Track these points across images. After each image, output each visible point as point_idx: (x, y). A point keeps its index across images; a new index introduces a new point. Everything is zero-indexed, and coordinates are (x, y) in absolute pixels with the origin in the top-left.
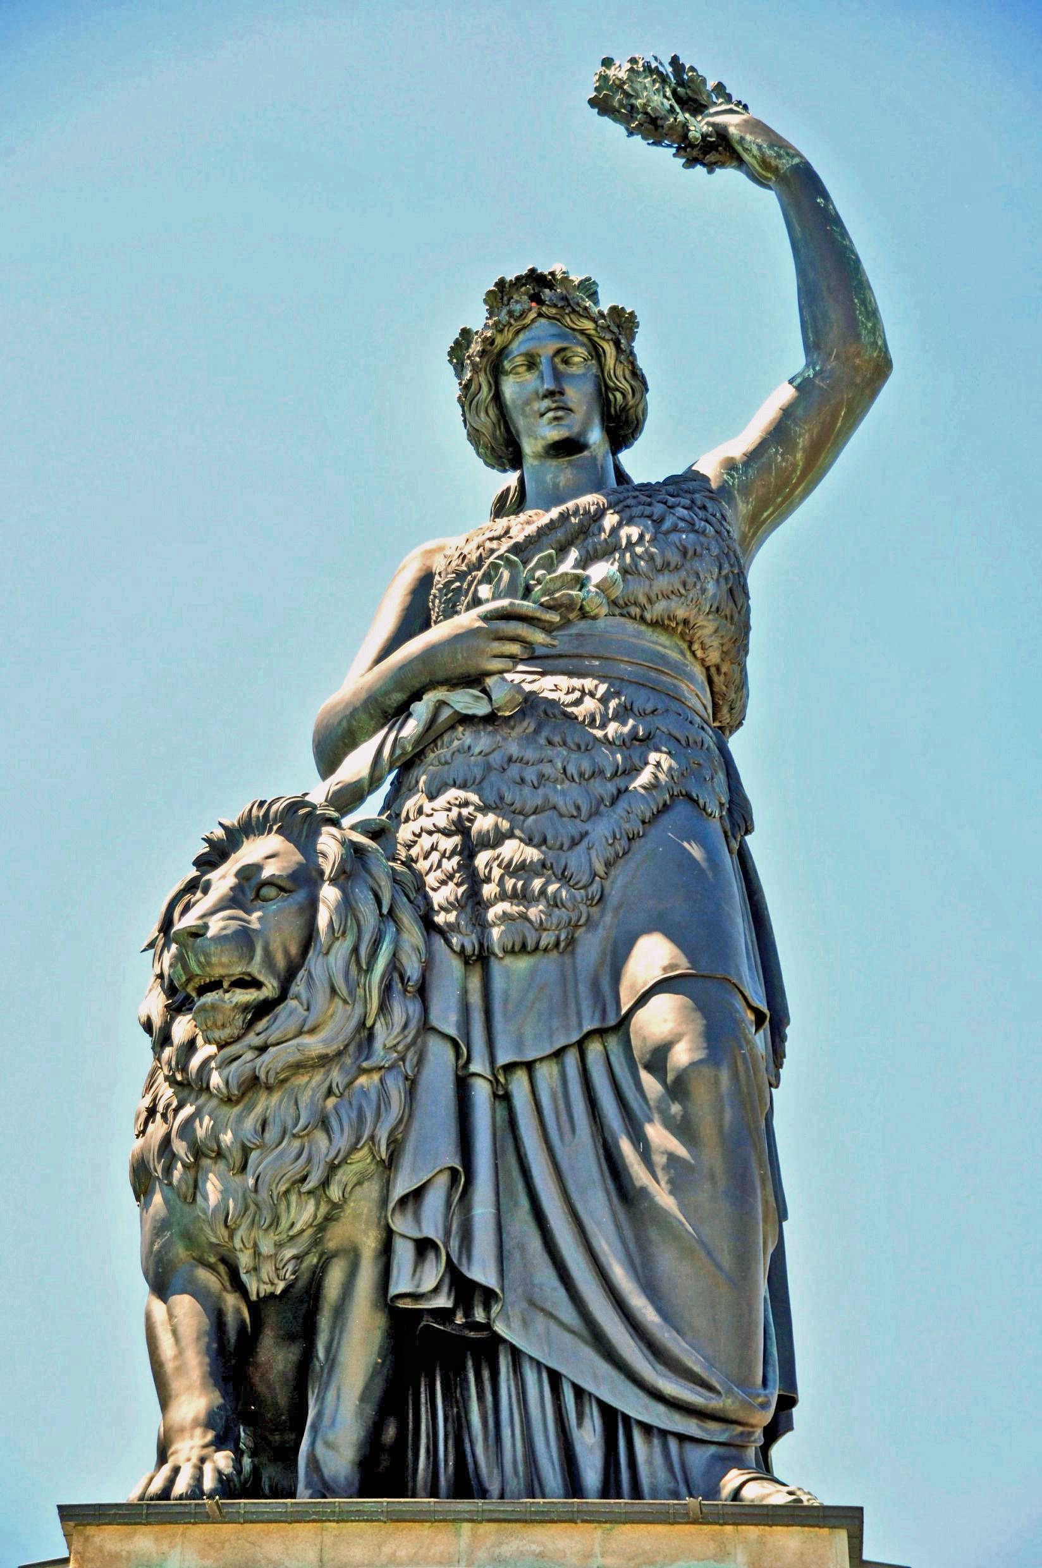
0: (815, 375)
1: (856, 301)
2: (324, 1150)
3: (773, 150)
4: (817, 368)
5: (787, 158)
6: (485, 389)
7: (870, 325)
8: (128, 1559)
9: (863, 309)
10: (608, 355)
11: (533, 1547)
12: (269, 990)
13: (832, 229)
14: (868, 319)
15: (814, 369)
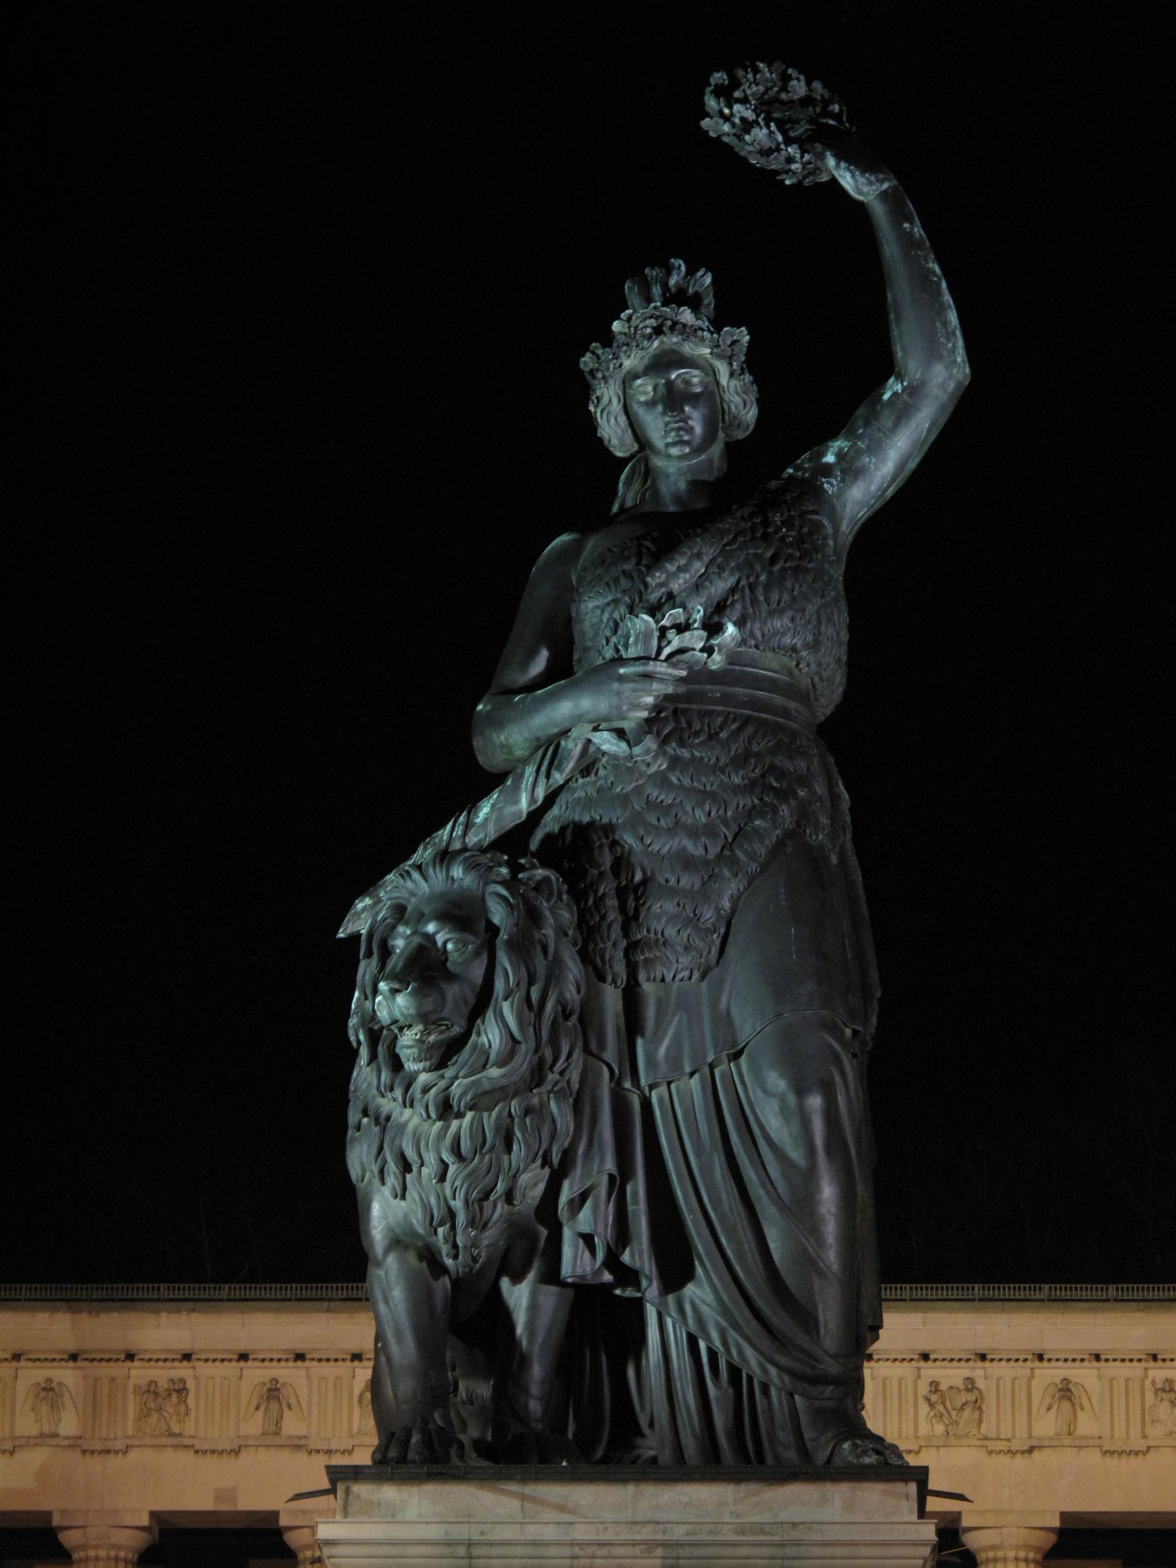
0: (904, 389)
1: (938, 324)
2: (506, 1165)
3: (865, 177)
4: (905, 384)
5: (877, 184)
6: (615, 401)
7: (950, 345)
8: (379, 1505)
9: (943, 331)
10: (722, 374)
11: (682, 1498)
12: (457, 1030)
13: (917, 254)
14: (948, 340)
15: (902, 385)
